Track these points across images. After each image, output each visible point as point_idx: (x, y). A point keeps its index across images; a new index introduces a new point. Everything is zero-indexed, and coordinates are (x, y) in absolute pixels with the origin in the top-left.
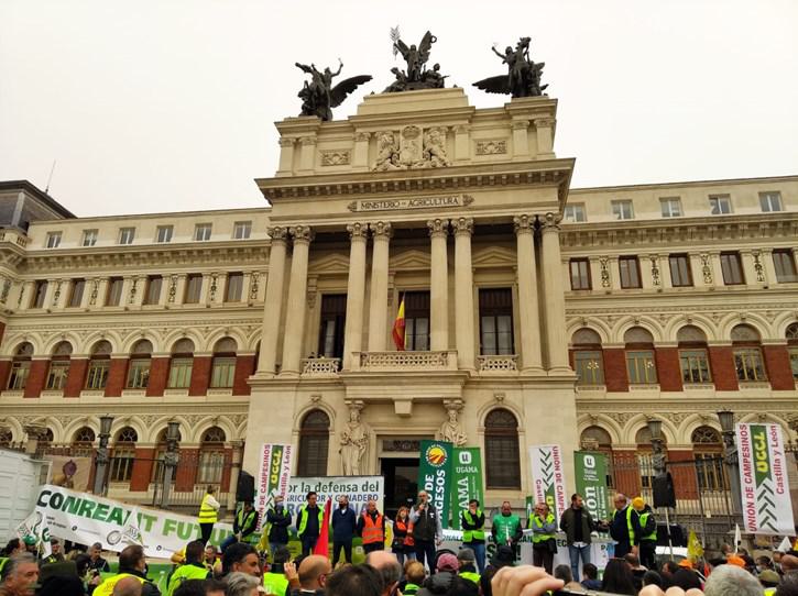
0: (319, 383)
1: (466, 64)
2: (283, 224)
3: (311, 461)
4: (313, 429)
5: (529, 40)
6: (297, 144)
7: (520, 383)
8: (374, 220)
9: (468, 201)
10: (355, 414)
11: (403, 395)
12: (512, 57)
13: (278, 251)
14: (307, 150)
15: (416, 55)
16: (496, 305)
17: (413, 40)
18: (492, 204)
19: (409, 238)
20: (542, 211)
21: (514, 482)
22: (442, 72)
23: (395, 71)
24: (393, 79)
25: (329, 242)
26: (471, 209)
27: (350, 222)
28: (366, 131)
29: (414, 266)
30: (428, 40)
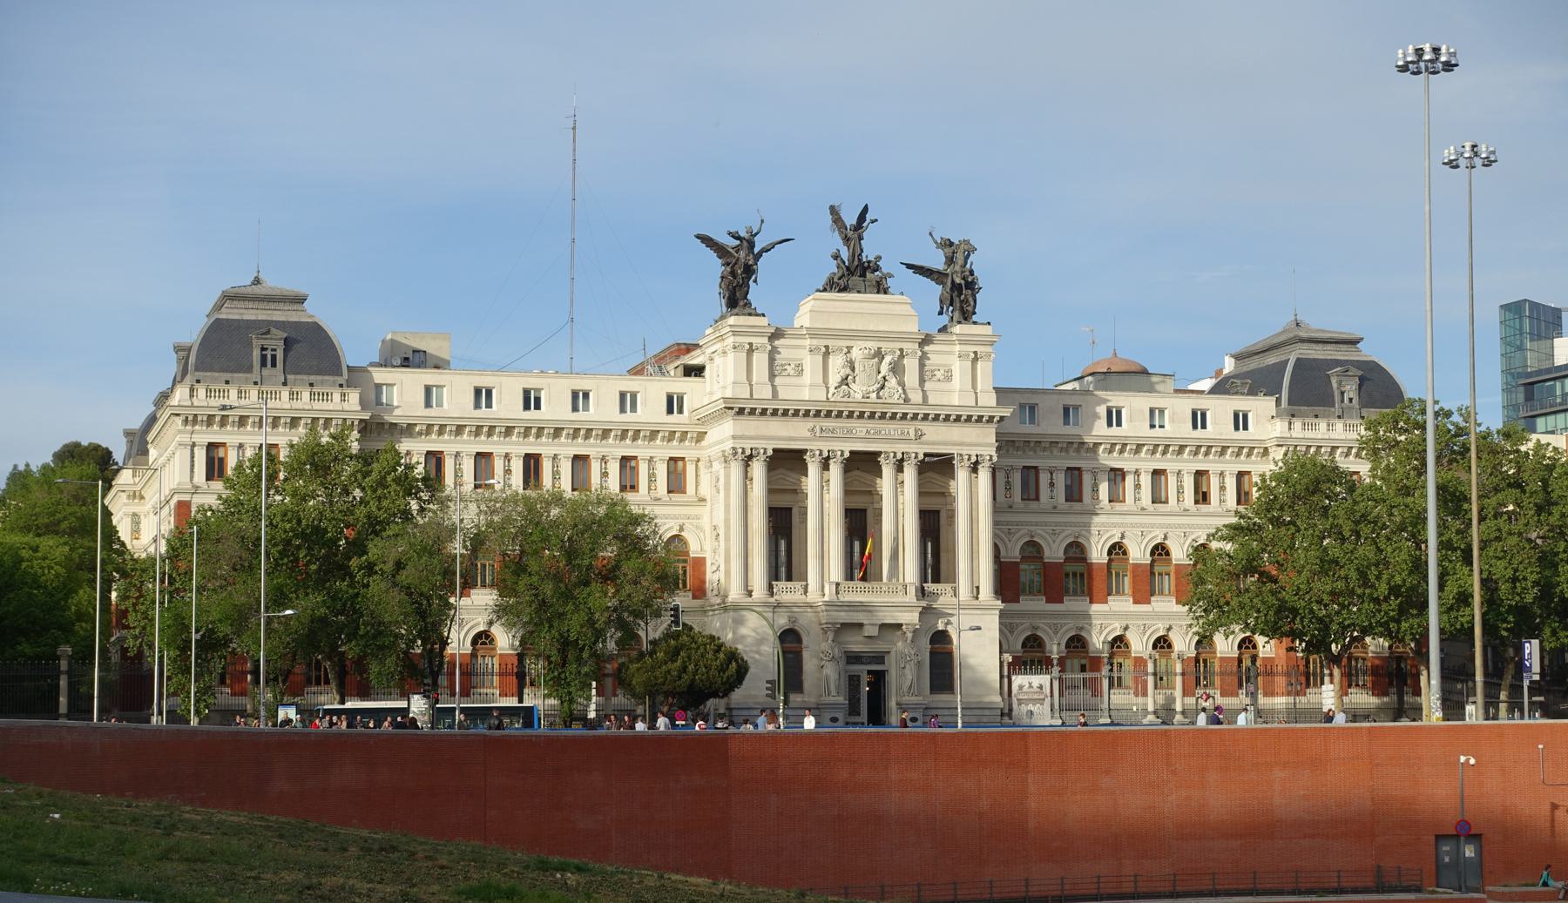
2: (748, 445)
9: (919, 436)
17: (850, 219)
18: (939, 438)
19: (862, 465)
23: (836, 257)
25: (787, 462)
27: (813, 446)
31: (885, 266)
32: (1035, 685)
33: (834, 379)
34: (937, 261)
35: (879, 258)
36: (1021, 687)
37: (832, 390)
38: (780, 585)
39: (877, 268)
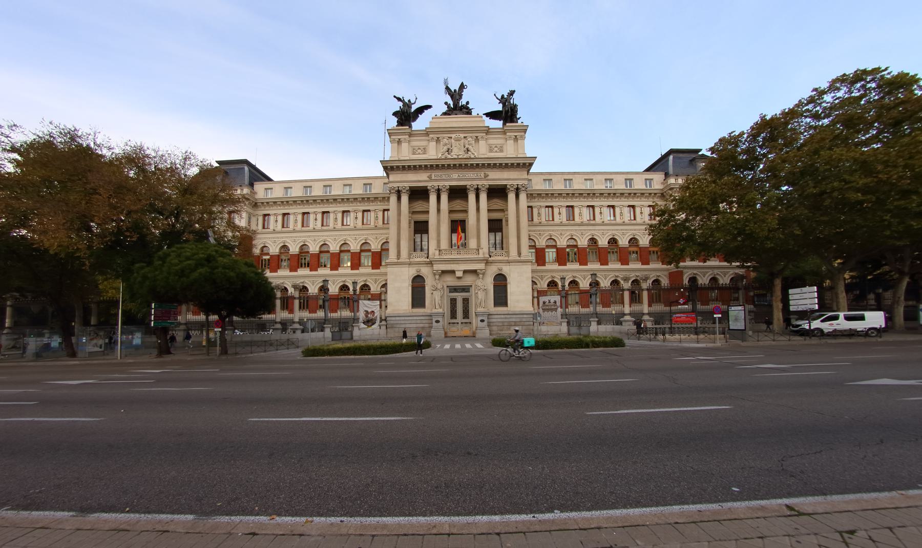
0: (419, 263)
1: (482, 101)
2: (396, 185)
3: (418, 298)
4: (418, 285)
5: (514, 91)
6: (399, 142)
7: (509, 262)
8: (441, 184)
10: (437, 277)
11: (460, 268)
12: (503, 100)
13: (393, 198)
14: (405, 146)
15: (456, 95)
16: (496, 226)
17: (454, 87)
18: (498, 177)
19: (458, 193)
20: (520, 183)
21: (505, 304)
22: (470, 106)
23: (446, 103)
24: (445, 109)
25: (419, 194)
27: (429, 185)
28: (435, 136)
29: (458, 208)
30: (462, 87)
32: (552, 301)
34: (499, 107)
35: (468, 103)
36: (544, 303)
38: (414, 254)
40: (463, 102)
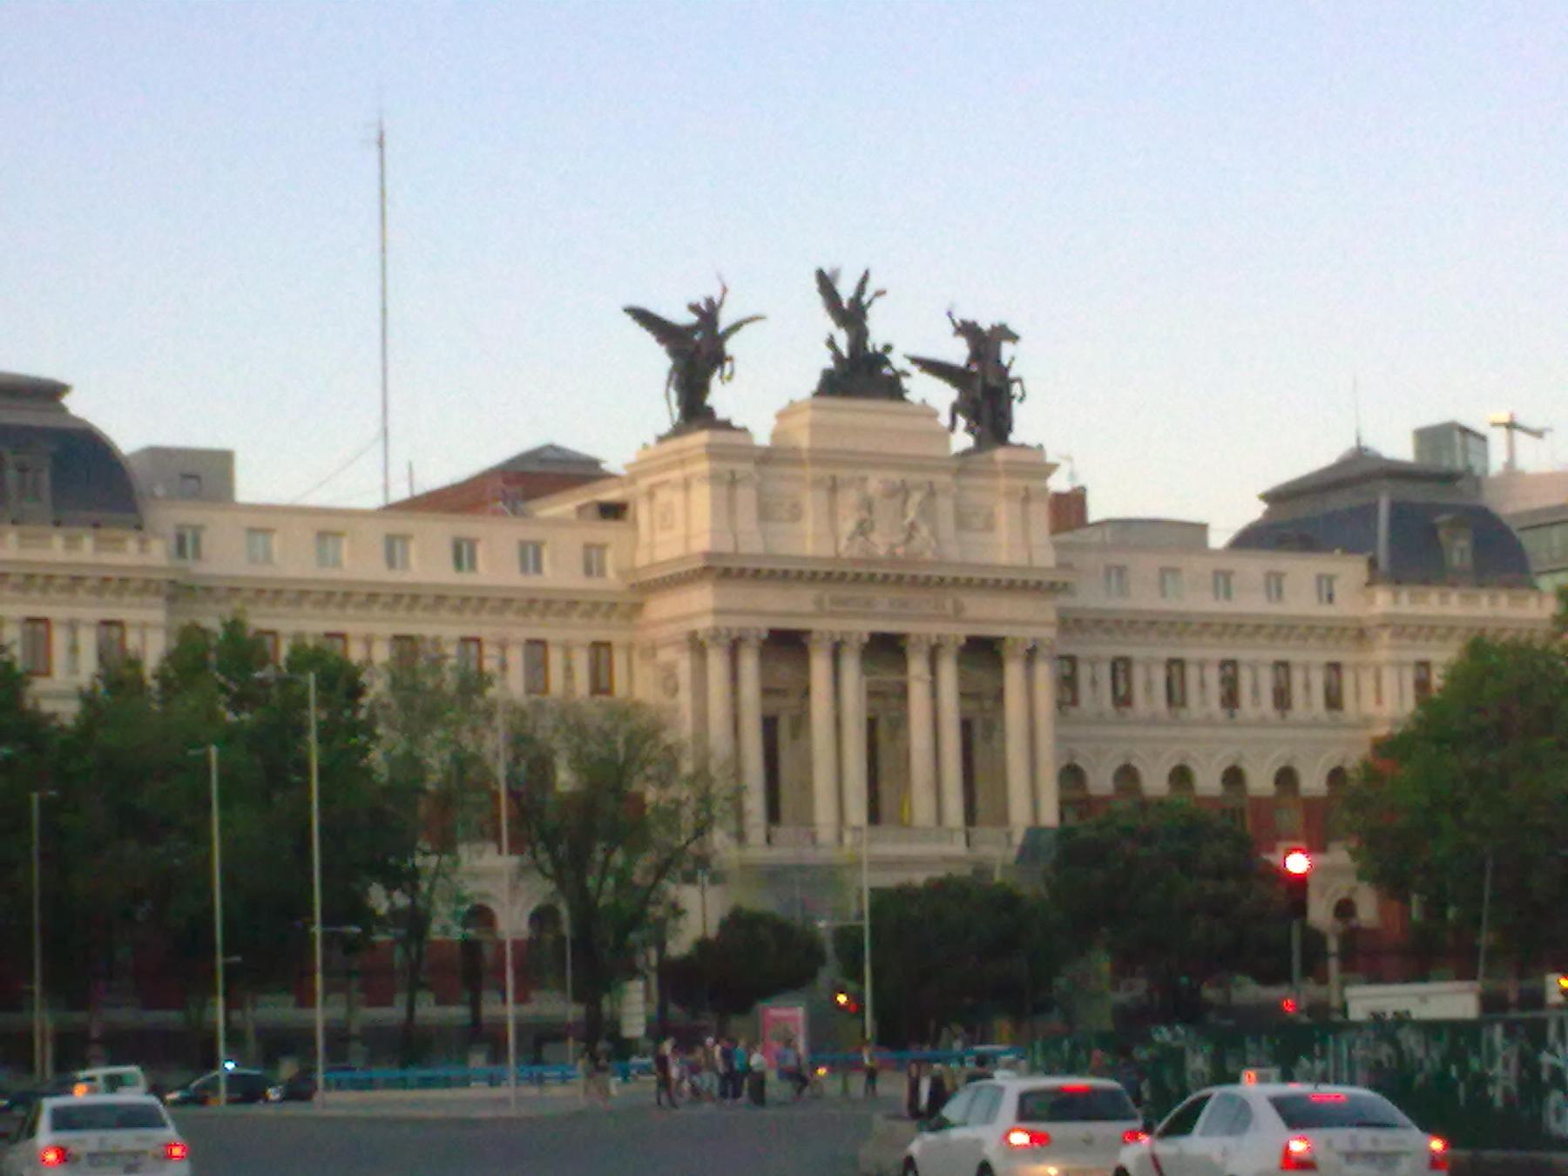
1: (910, 329)
2: (735, 623)
6: (734, 482)
14: (746, 496)
15: (851, 315)
23: (831, 343)
26: (966, 621)
31: (898, 361)
33: (848, 526)
34: (957, 352)
35: (888, 348)
37: (843, 542)
39: (887, 363)
40: (876, 341)
